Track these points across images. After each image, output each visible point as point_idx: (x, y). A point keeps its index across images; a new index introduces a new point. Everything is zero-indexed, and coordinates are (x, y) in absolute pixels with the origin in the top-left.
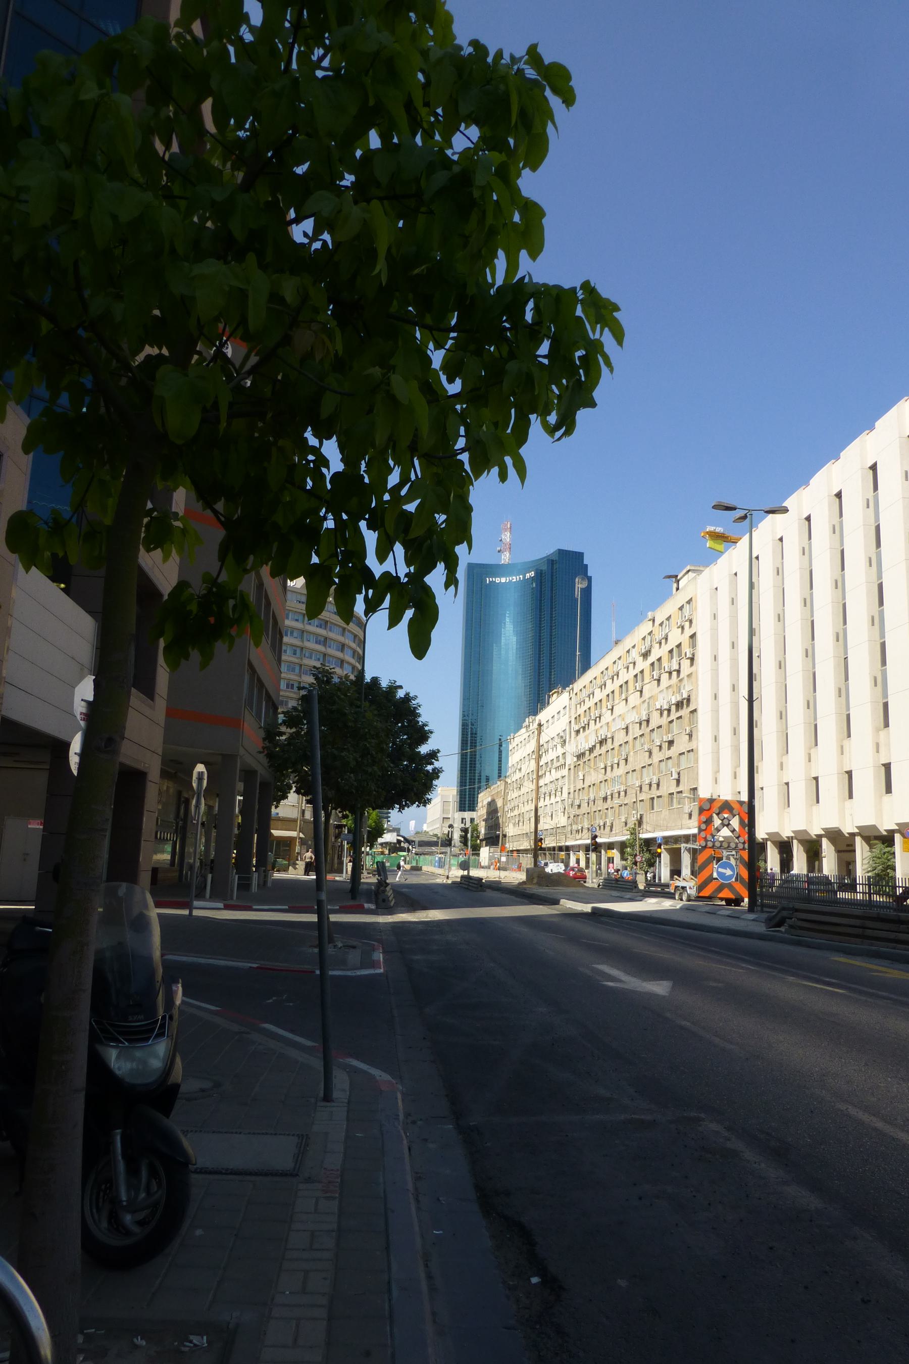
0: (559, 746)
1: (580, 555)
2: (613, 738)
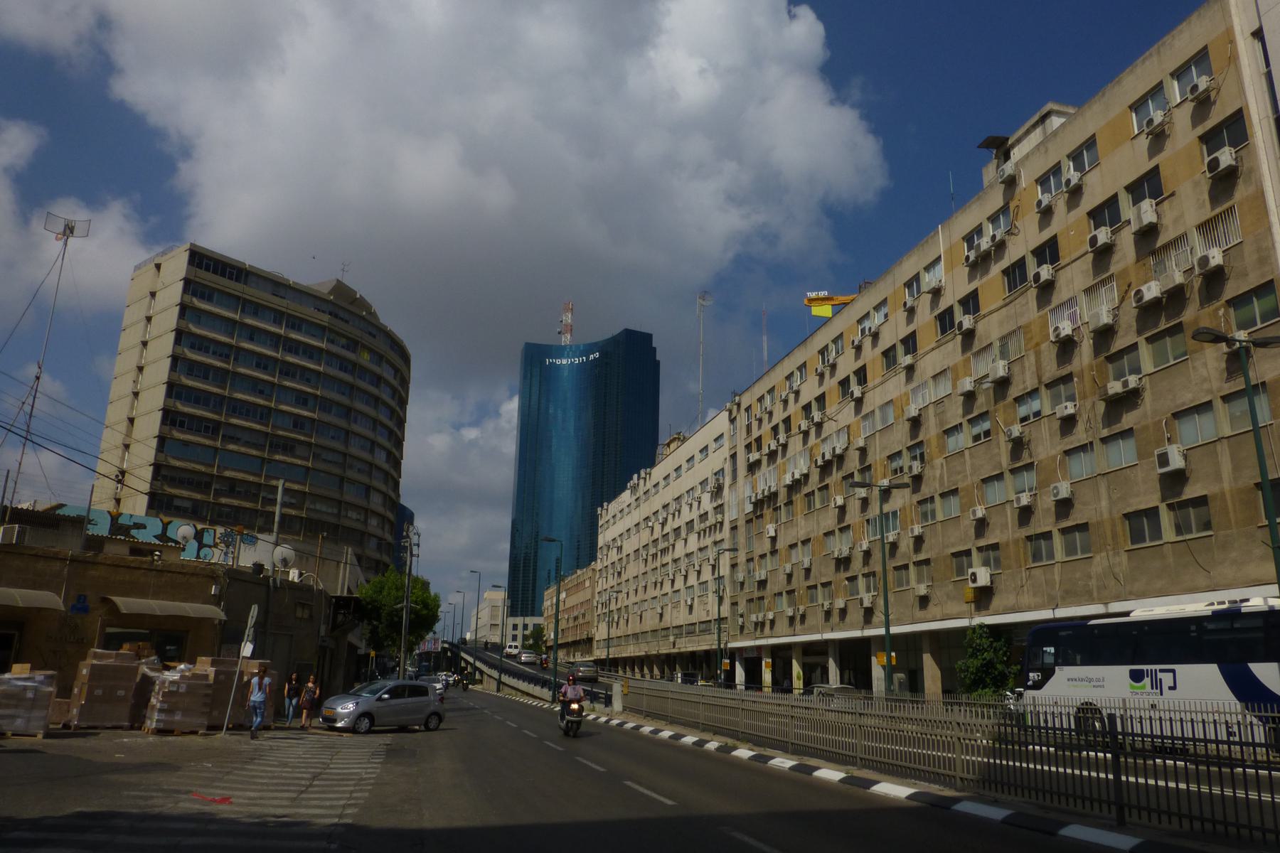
0: (706, 498)
1: (648, 337)
2: (863, 451)
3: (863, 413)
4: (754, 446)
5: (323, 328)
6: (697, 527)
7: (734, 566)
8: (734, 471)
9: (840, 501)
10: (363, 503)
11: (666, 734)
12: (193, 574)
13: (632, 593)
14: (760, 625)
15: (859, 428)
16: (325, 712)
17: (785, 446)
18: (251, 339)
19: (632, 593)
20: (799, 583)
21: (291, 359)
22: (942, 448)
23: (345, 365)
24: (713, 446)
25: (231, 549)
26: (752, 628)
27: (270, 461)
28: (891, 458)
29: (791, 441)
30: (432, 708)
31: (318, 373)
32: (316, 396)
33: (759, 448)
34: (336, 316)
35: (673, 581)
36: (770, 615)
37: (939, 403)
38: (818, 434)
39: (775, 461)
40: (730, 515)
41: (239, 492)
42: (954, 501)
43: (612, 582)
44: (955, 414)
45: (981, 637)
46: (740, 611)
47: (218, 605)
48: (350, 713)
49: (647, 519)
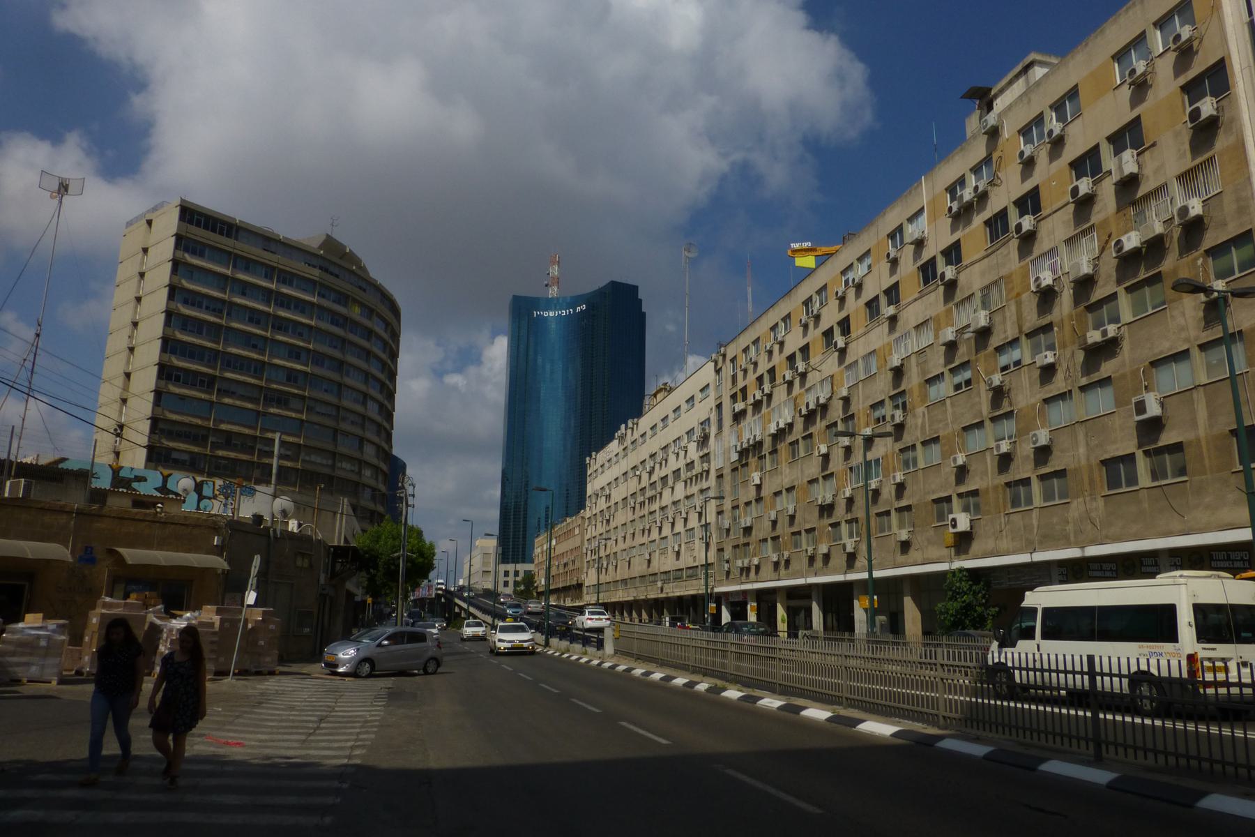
0: (692, 447)
1: (634, 289)
2: (846, 401)
3: (847, 363)
4: (739, 396)
5: (314, 282)
6: (683, 476)
7: (720, 513)
8: (720, 421)
9: (824, 450)
10: (357, 454)
11: (657, 676)
12: (195, 526)
13: (620, 540)
14: (745, 571)
15: (842, 379)
16: (327, 657)
17: (770, 396)
18: (244, 294)
19: (620, 540)
20: (784, 529)
21: (282, 313)
22: (924, 397)
23: (336, 319)
24: (699, 396)
25: (230, 500)
26: (737, 572)
27: (265, 414)
28: (874, 407)
29: (776, 390)
30: (430, 654)
31: (310, 327)
32: (308, 350)
33: (745, 398)
34: (326, 270)
35: (660, 528)
36: (756, 561)
37: (921, 352)
38: (802, 383)
39: (760, 411)
40: (715, 465)
41: (236, 445)
42: (935, 449)
43: (601, 529)
44: (937, 364)
45: (961, 580)
46: (726, 557)
47: (221, 555)
48: (349, 661)
49: (634, 468)
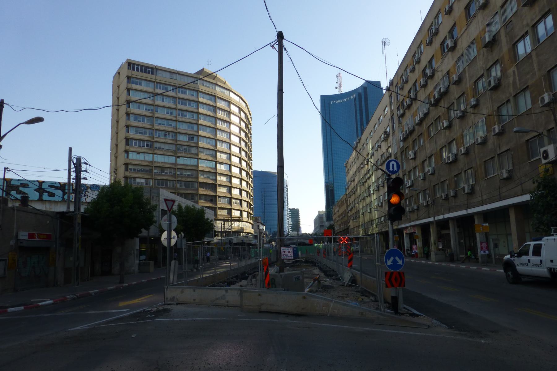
17: (415, 99)
